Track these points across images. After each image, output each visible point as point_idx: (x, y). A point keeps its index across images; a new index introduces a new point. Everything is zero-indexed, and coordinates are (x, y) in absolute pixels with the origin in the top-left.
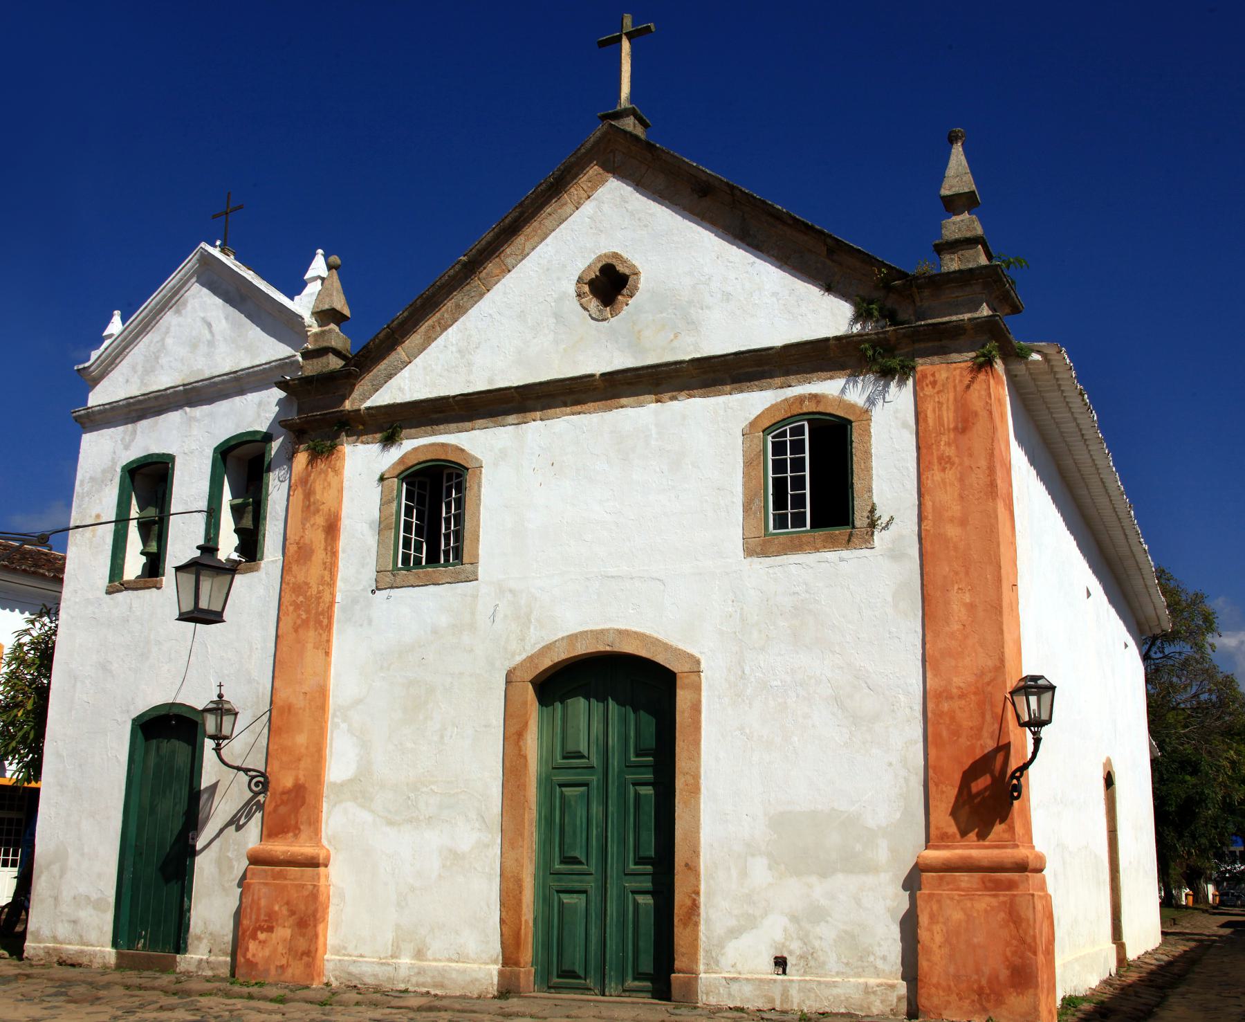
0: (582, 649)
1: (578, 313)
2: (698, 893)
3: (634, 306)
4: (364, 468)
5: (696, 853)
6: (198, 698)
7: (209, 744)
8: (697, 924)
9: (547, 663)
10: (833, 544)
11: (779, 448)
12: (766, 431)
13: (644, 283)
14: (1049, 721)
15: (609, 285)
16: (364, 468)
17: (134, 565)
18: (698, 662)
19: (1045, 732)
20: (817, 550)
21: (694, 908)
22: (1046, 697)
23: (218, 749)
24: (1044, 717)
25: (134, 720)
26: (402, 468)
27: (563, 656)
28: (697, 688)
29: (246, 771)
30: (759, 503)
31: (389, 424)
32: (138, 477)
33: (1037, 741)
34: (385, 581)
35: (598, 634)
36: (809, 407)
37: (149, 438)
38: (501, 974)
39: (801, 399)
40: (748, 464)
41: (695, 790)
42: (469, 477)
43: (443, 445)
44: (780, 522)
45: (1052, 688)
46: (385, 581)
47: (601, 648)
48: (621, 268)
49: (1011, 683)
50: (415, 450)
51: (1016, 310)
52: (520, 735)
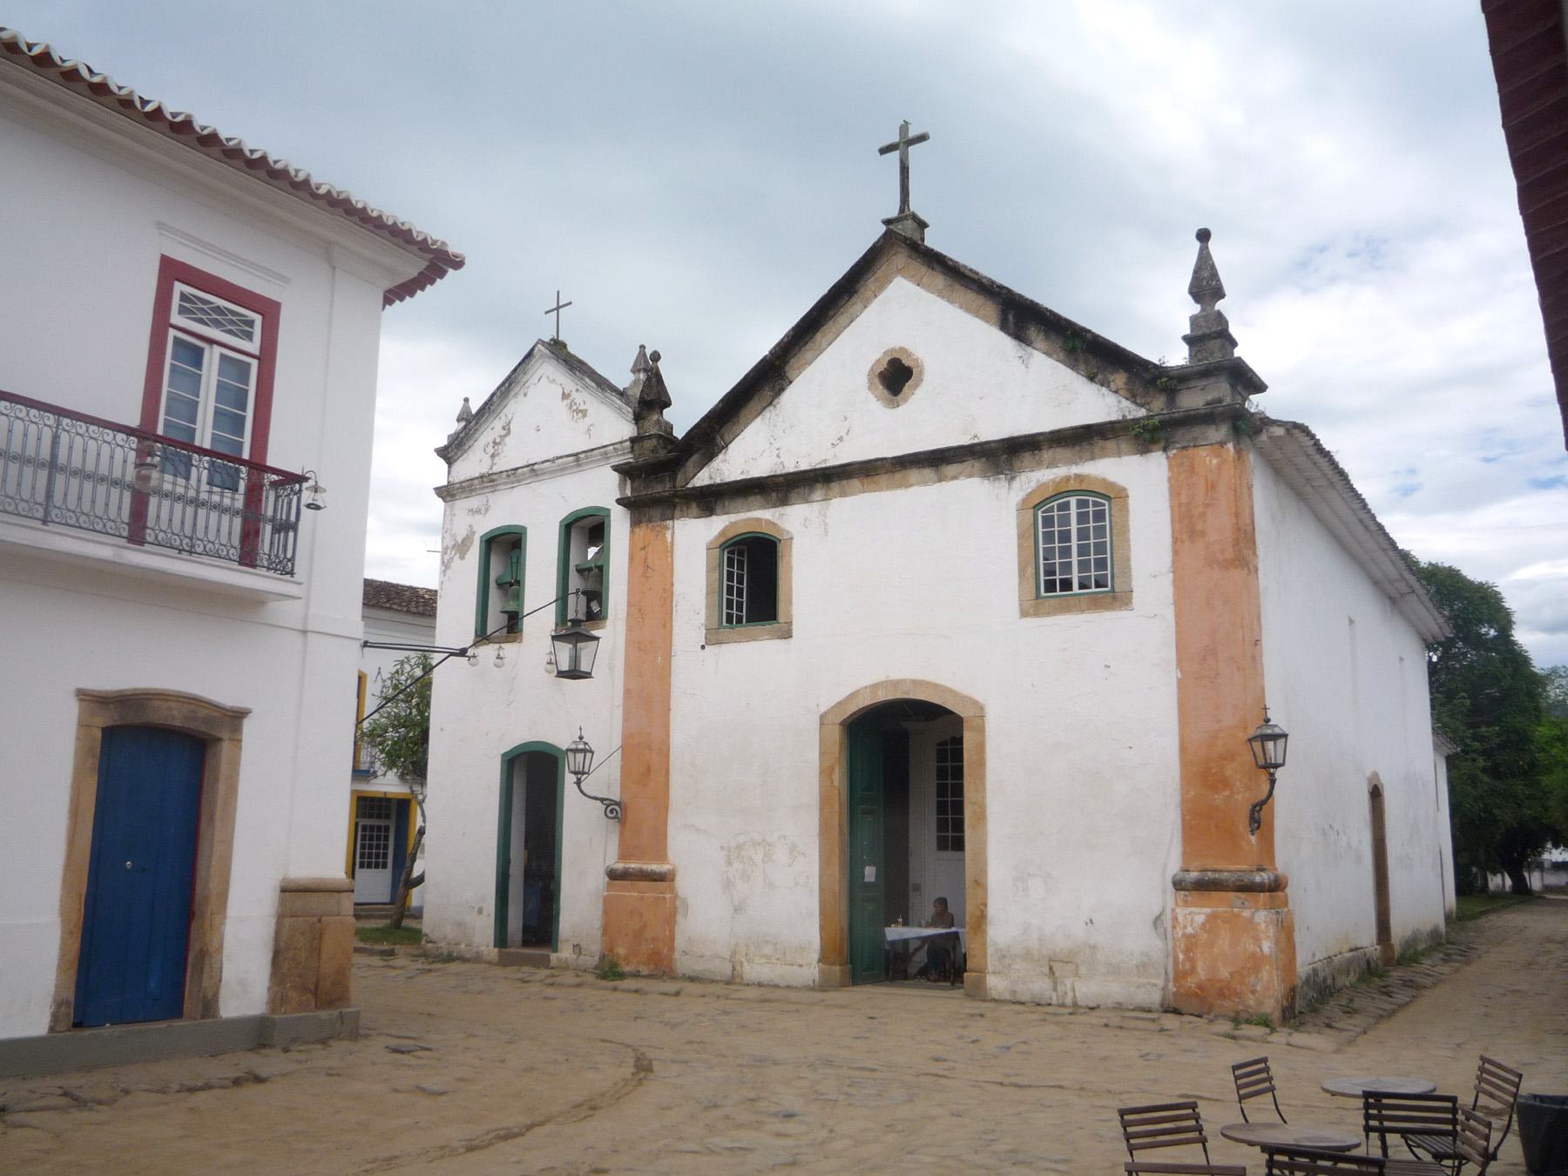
0: (883, 696)
1: (871, 404)
2: (985, 905)
3: (918, 398)
4: (694, 540)
5: (984, 872)
6: (561, 739)
7: (569, 779)
8: (985, 932)
9: (853, 708)
10: (1096, 604)
11: (1048, 522)
12: (1036, 507)
13: (928, 377)
14: (1282, 765)
15: (896, 377)
16: (694, 540)
17: (495, 621)
18: (982, 708)
19: (1279, 773)
20: (1083, 611)
21: (981, 919)
22: (1281, 742)
23: (578, 783)
24: (1280, 761)
25: (504, 755)
26: (723, 540)
27: (868, 702)
28: (981, 730)
29: (602, 800)
30: (1030, 570)
31: (711, 499)
32: (493, 546)
33: (1273, 782)
34: (713, 638)
35: (896, 684)
36: (1073, 485)
37: (502, 512)
38: (821, 972)
39: (1067, 479)
40: (1021, 536)
41: (981, 816)
42: (780, 548)
43: (758, 520)
44: (1050, 586)
45: (1285, 736)
46: (713, 638)
47: (899, 696)
48: (906, 362)
49: (1252, 732)
50: (733, 524)
51: (1259, 387)
52: (832, 770)
